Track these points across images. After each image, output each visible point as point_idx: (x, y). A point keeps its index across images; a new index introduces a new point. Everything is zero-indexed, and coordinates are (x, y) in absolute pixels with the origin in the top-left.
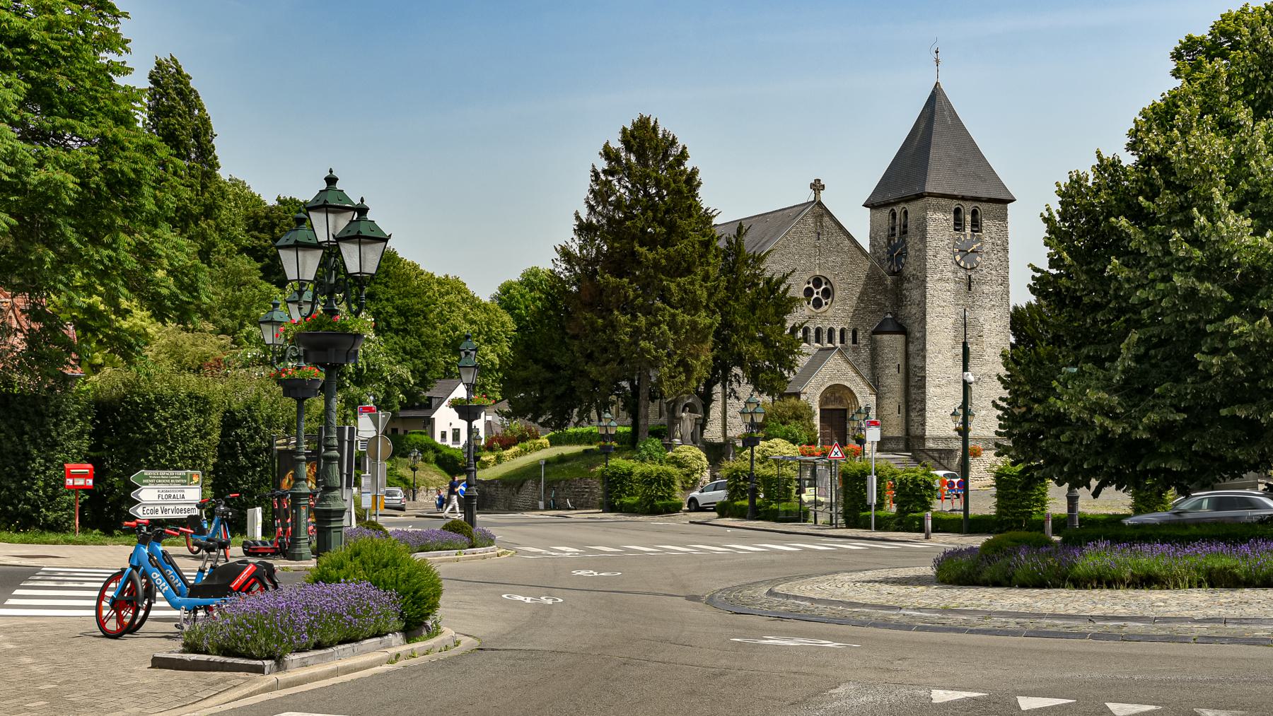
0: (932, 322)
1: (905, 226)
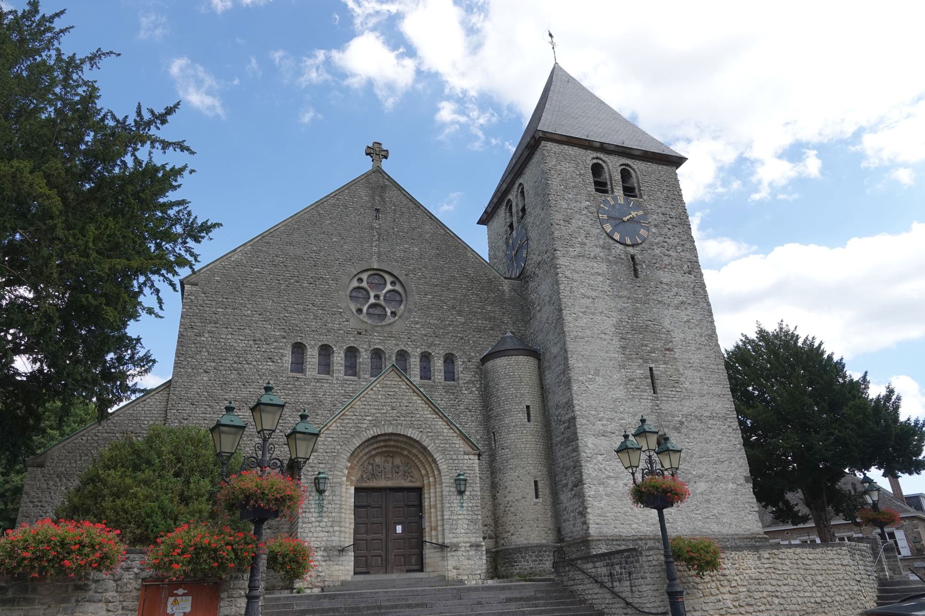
0: (576, 320)
1: (524, 210)
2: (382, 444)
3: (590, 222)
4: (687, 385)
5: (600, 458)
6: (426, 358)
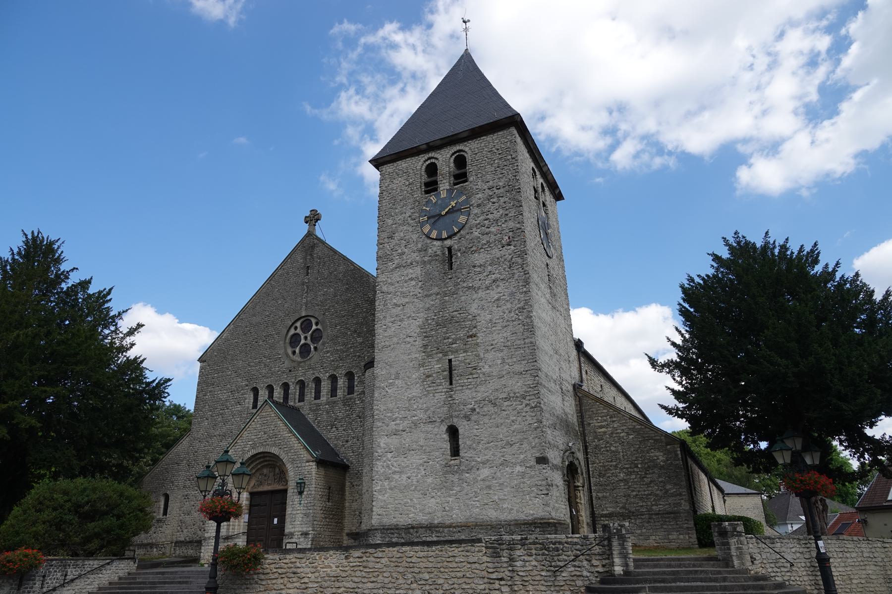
3: (410, 229)
4: (486, 369)
5: (389, 455)
6: (334, 379)
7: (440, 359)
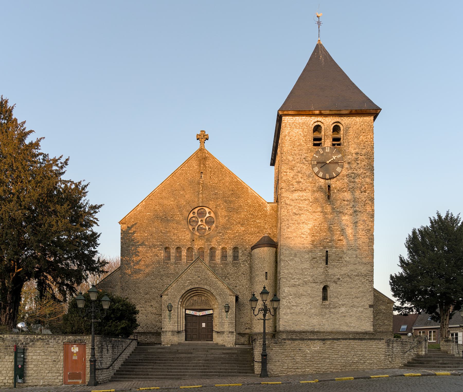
2: (195, 292)
5: (290, 297)
7: (321, 250)
